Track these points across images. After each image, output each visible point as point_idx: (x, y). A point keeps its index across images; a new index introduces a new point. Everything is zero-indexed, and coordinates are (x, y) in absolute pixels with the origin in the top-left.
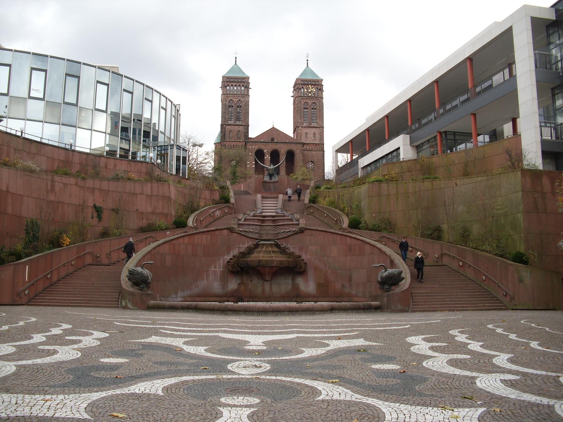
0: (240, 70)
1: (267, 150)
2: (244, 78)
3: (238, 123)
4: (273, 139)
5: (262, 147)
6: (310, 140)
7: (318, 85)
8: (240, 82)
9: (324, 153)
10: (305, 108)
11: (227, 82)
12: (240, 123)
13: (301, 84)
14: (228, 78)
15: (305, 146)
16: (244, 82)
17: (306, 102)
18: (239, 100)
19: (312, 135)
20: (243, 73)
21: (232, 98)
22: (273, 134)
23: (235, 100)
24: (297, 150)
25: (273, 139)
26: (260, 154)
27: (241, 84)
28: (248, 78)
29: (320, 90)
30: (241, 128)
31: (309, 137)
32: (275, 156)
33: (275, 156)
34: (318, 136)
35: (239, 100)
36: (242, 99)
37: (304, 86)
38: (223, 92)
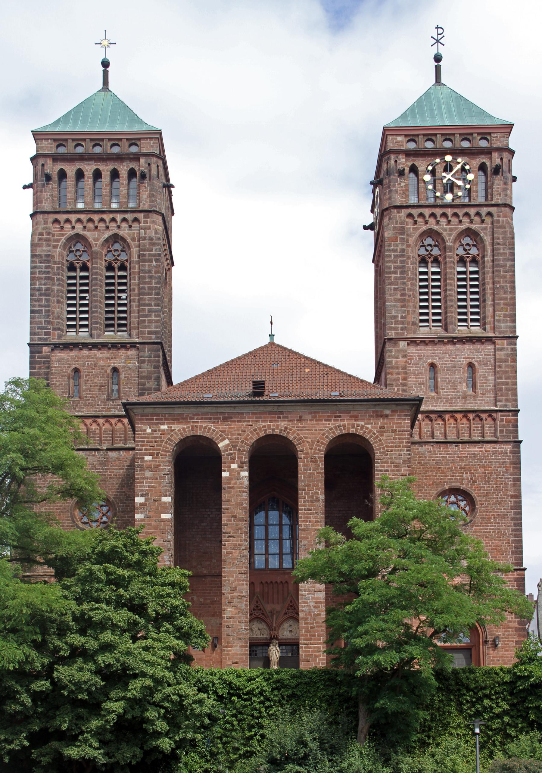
0: (120, 107)
1: (235, 440)
2: (134, 140)
3: (109, 336)
4: (259, 389)
5: (206, 428)
6: (452, 393)
7: (488, 152)
8: (119, 158)
9: (517, 453)
10: (423, 261)
11: (56, 158)
12: (122, 336)
13: (408, 154)
14: (60, 140)
15: (425, 426)
16: (136, 158)
17: (430, 233)
18: (116, 238)
19: (462, 375)
20: (135, 119)
21: (79, 228)
22: (269, 378)
23: (97, 237)
24: (383, 435)
25: (259, 389)
26: (196, 466)
27: (123, 169)
28: (157, 136)
29: (497, 170)
30: (124, 359)
31: (444, 378)
32: (273, 467)
33: (273, 467)
34: (486, 378)
35: (116, 238)
36: (124, 232)
37: (422, 164)
38: (37, 202)
